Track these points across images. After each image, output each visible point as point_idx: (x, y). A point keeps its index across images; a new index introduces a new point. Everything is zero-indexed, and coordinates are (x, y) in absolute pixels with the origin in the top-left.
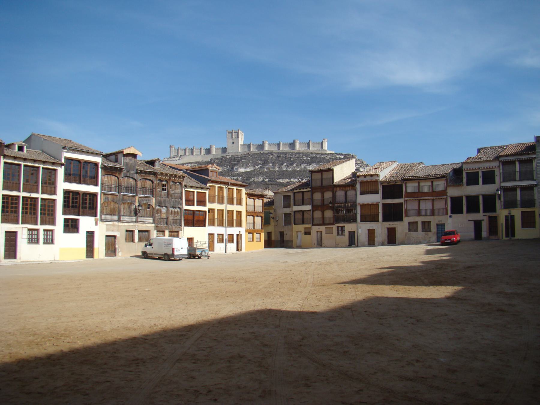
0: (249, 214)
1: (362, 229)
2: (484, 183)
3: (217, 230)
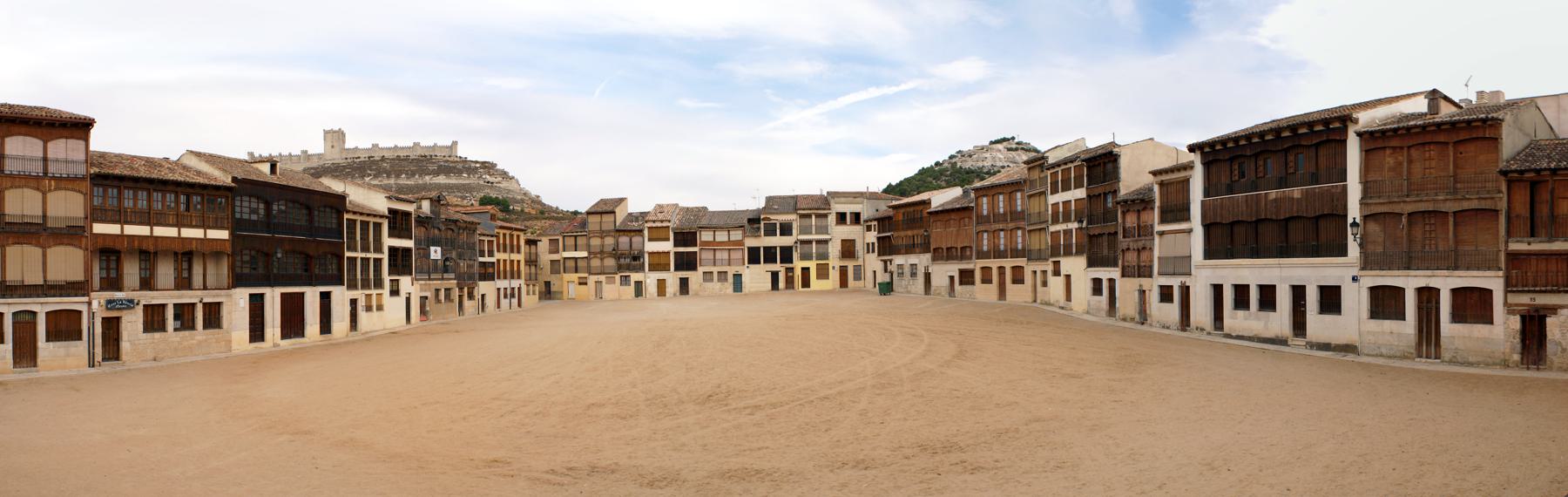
1: (650, 279)
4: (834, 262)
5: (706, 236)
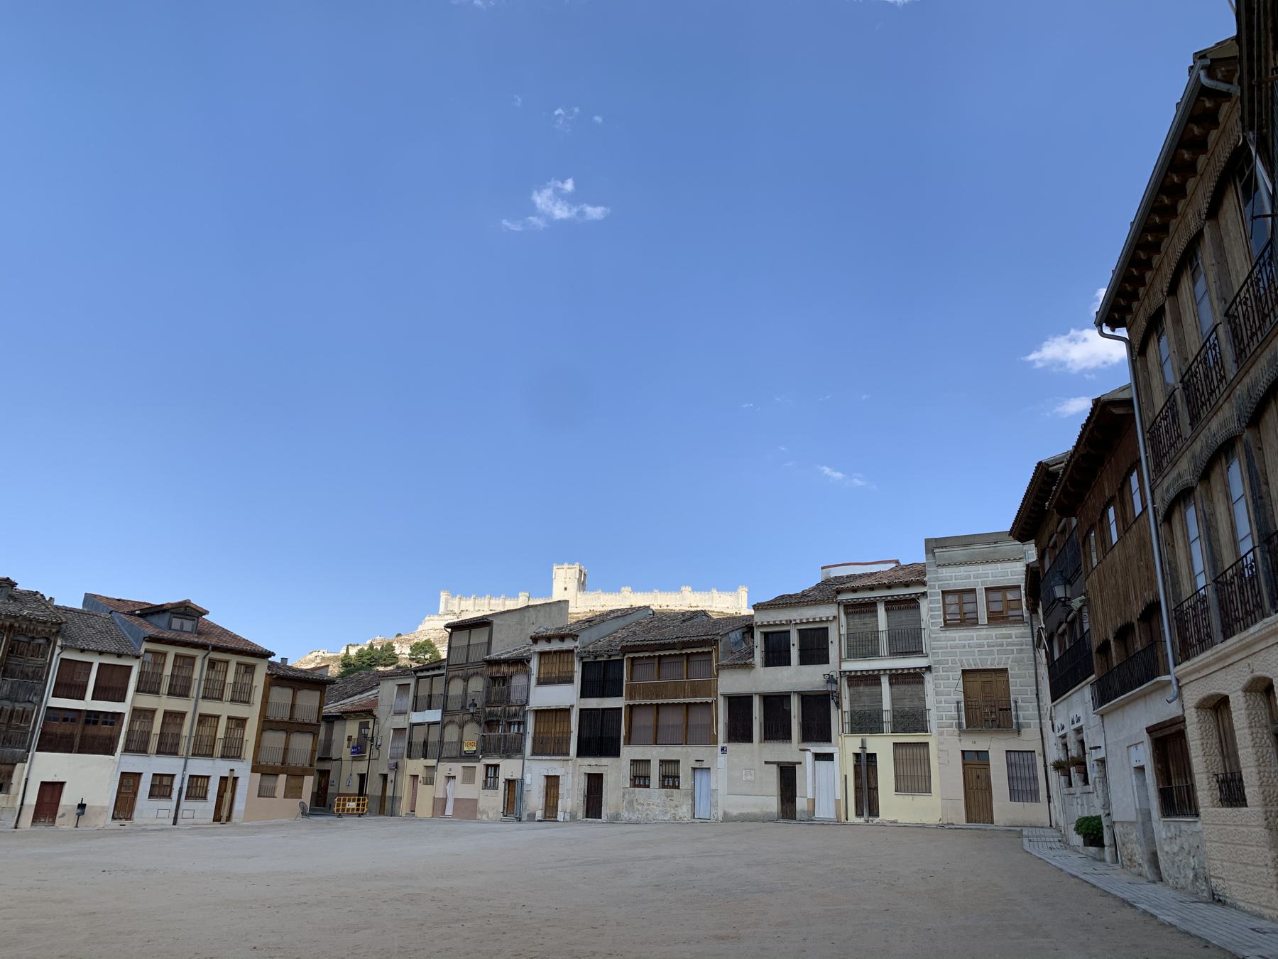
0: (267, 724)
1: (532, 772)
2: (804, 660)
3: (149, 766)
4: (945, 746)
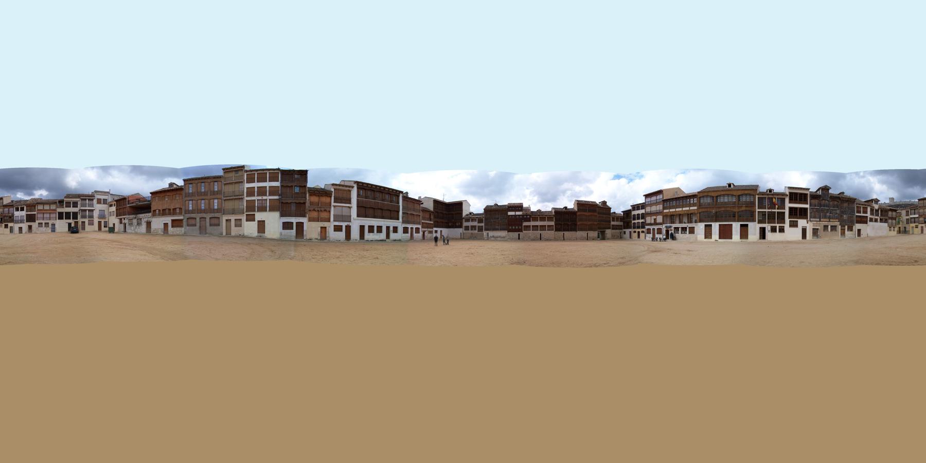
1: (16, 227)
4: (96, 220)
5: (40, 207)
